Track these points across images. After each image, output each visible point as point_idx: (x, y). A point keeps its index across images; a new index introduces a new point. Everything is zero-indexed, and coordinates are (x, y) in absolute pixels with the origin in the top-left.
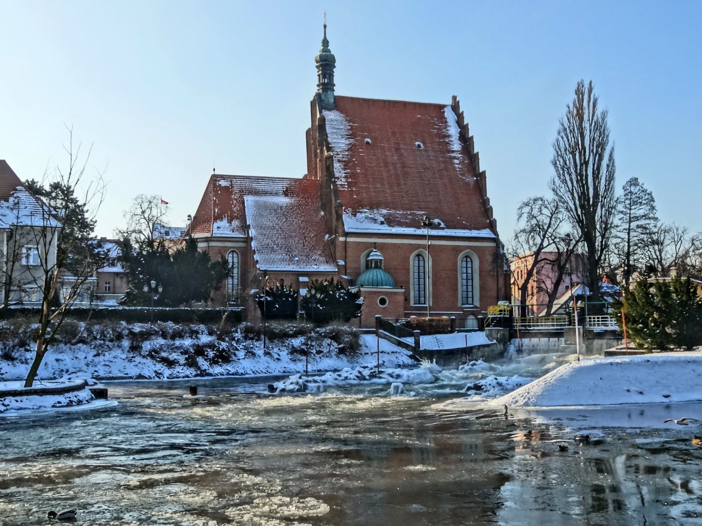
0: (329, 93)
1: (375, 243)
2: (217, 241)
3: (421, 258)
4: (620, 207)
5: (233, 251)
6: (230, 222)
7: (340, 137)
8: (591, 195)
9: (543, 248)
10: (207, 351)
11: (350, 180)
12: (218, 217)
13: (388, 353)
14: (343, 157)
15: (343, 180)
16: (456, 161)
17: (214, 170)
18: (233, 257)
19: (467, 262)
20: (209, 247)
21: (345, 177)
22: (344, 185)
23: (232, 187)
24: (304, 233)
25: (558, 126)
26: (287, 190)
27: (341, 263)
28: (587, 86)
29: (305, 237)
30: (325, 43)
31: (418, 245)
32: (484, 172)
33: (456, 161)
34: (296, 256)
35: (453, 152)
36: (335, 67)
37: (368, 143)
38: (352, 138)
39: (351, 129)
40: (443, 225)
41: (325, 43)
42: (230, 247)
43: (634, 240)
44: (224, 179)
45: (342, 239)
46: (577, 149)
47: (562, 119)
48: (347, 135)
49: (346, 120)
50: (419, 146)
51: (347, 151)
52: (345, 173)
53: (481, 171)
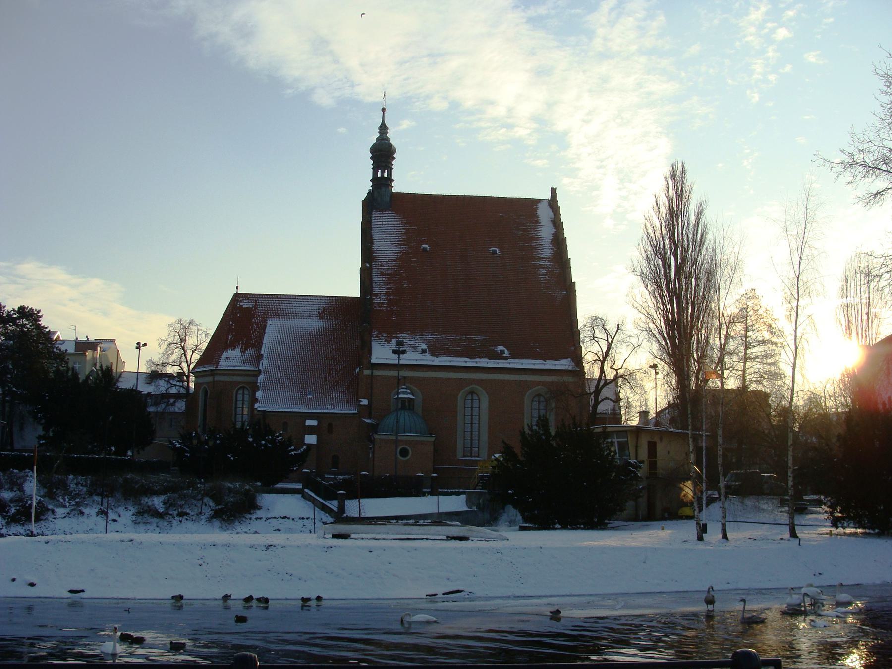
2: (238, 375)
3: (475, 397)
5: (243, 387)
6: (243, 351)
7: (389, 243)
10: (10, 506)
11: (391, 297)
12: (233, 346)
13: (293, 519)
14: (388, 269)
15: (383, 297)
16: (542, 270)
17: (237, 288)
18: (243, 394)
19: (472, 400)
20: (214, 381)
21: (386, 294)
22: (383, 303)
23: (256, 308)
24: (330, 365)
26: (323, 312)
27: (365, 402)
29: (330, 370)
30: (383, 128)
31: (470, 379)
32: (575, 283)
33: (543, 271)
34: (310, 394)
35: (541, 259)
36: (394, 158)
37: (425, 250)
38: (404, 245)
39: (405, 234)
40: (507, 353)
41: (383, 128)
42: (240, 382)
45: (367, 372)
48: (399, 241)
49: (402, 222)
50: (494, 252)
51: (395, 260)
52: (387, 289)
53: (573, 282)
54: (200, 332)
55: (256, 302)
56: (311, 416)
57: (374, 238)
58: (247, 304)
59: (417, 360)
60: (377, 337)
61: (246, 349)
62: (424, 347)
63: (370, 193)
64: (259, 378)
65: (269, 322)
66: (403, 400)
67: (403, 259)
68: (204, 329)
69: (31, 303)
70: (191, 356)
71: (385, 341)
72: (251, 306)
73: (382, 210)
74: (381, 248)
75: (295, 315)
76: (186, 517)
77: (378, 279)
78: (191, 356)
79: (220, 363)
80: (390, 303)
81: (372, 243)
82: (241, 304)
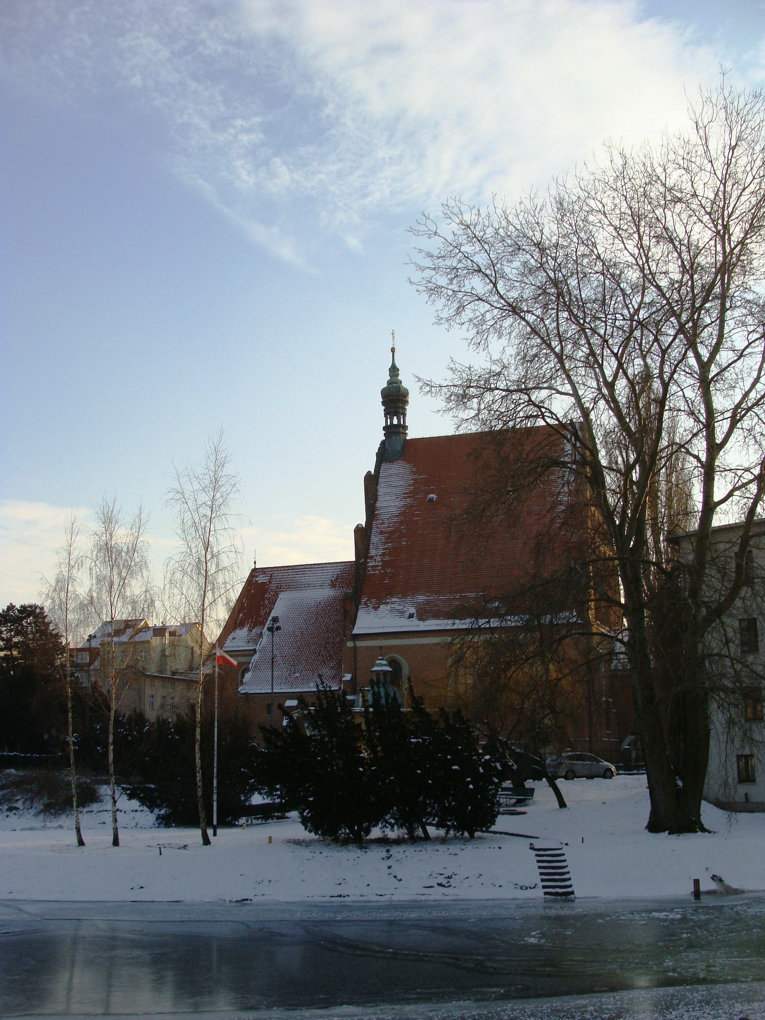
1: (381, 647)
11: (387, 558)
13: (125, 812)
14: (389, 527)
17: (255, 563)
21: (383, 555)
22: (378, 566)
24: (328, 638)
26: (336, 580)
30: (394, 370)
37: (431, 500)
38: (410, 497)
39: (413, 485)
41: (394, 370)
44: (264, 573)
45: (350, 644)
48: (404, 494)
49: (411, 472)
52: (384, 549)
55: (271, 576)
56: (291, 696)
57: (379, 493)
58: (263, 578)
59: (401, 627)
60: (366, 604)
61: (254, 628)
62: (413, 610)
63: (383, 443)
64: (253, 658)
65: (281, 596)
66: (378, 673)
67: (406, 515)
71: (373, 608)
72: (266, 581)
73: (392, 462)
74: (385, 504)
75: (308, 586)
76: (14, 811)
77: (377, 539)
79: (225, 645)
80: (385, 564)
81: (376, 500)
82: (257, 579)
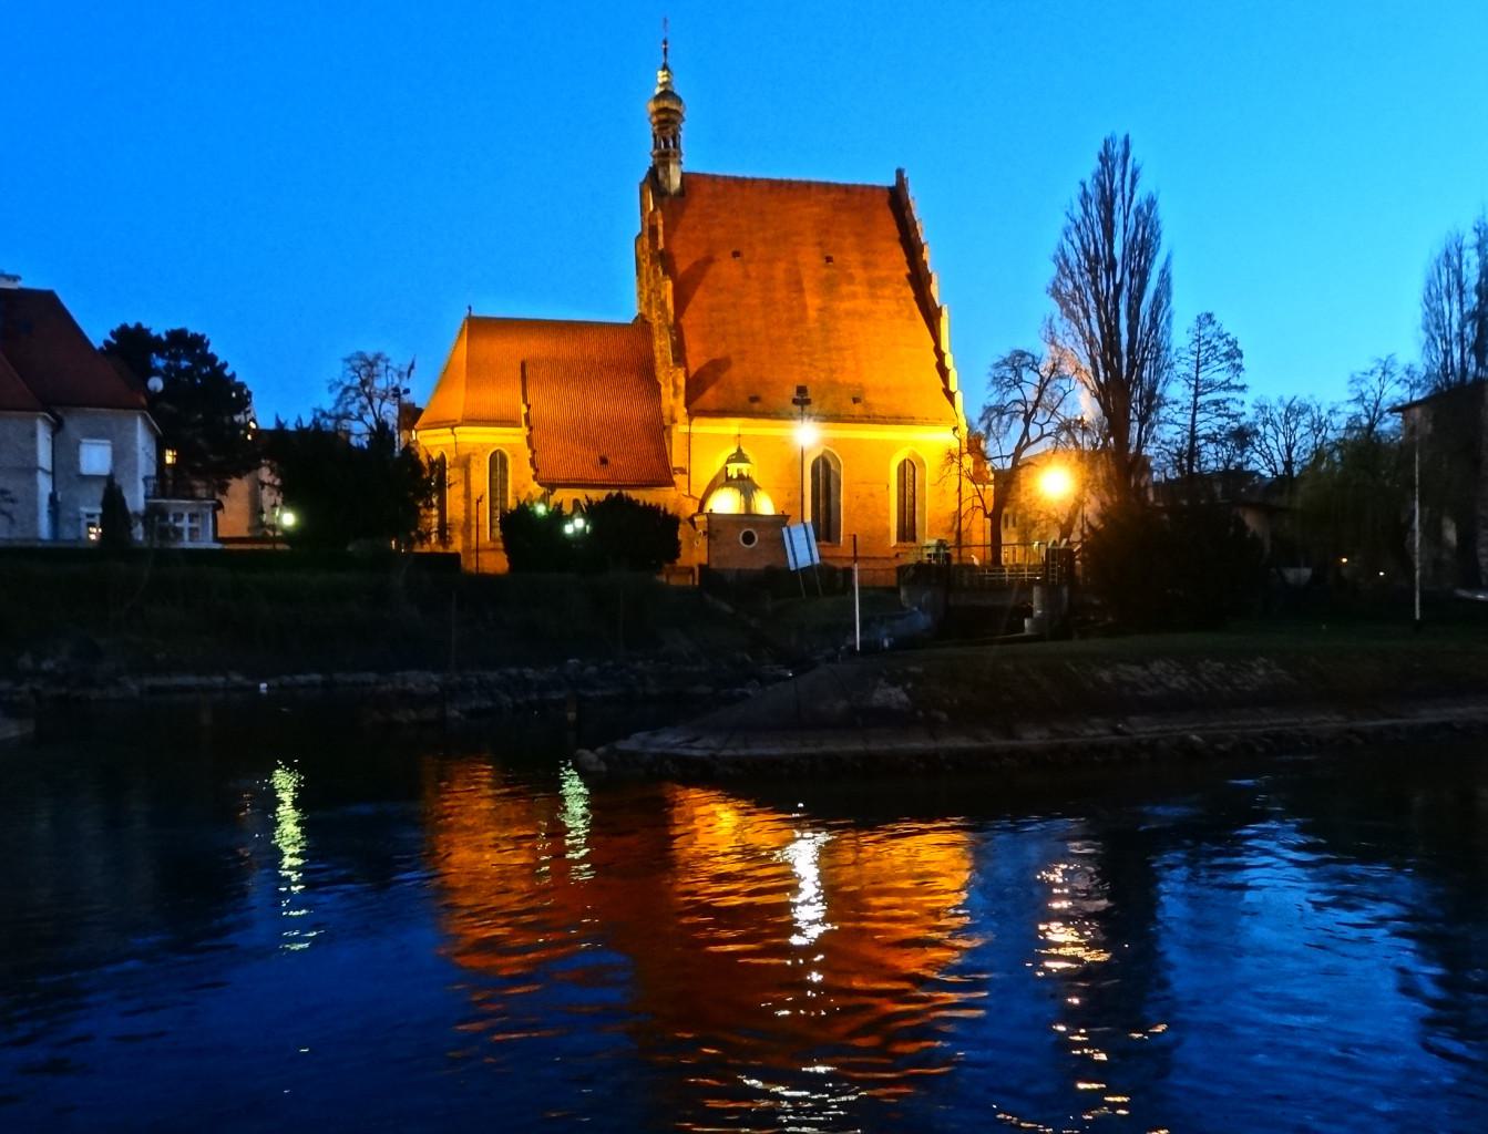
0: (672, 167)
4: (1181, 368)
8: (1124, 348)
9: (1029, 444)
17: (470, 308)
25: (1063, 221)
28: (1118, 149)
42: (494, 444)
43: (1203, 429)
46: (1097, 263)
47: (1072, 208)
54: (390, 371)
63: (653, 172)
68: (395, 366)
69: (193, 328)
70: (380, 406)
78: (380, 406)
